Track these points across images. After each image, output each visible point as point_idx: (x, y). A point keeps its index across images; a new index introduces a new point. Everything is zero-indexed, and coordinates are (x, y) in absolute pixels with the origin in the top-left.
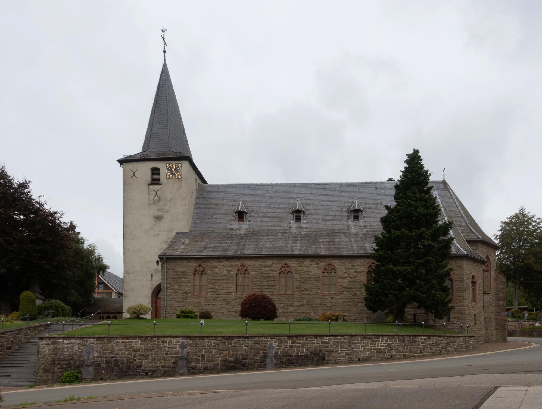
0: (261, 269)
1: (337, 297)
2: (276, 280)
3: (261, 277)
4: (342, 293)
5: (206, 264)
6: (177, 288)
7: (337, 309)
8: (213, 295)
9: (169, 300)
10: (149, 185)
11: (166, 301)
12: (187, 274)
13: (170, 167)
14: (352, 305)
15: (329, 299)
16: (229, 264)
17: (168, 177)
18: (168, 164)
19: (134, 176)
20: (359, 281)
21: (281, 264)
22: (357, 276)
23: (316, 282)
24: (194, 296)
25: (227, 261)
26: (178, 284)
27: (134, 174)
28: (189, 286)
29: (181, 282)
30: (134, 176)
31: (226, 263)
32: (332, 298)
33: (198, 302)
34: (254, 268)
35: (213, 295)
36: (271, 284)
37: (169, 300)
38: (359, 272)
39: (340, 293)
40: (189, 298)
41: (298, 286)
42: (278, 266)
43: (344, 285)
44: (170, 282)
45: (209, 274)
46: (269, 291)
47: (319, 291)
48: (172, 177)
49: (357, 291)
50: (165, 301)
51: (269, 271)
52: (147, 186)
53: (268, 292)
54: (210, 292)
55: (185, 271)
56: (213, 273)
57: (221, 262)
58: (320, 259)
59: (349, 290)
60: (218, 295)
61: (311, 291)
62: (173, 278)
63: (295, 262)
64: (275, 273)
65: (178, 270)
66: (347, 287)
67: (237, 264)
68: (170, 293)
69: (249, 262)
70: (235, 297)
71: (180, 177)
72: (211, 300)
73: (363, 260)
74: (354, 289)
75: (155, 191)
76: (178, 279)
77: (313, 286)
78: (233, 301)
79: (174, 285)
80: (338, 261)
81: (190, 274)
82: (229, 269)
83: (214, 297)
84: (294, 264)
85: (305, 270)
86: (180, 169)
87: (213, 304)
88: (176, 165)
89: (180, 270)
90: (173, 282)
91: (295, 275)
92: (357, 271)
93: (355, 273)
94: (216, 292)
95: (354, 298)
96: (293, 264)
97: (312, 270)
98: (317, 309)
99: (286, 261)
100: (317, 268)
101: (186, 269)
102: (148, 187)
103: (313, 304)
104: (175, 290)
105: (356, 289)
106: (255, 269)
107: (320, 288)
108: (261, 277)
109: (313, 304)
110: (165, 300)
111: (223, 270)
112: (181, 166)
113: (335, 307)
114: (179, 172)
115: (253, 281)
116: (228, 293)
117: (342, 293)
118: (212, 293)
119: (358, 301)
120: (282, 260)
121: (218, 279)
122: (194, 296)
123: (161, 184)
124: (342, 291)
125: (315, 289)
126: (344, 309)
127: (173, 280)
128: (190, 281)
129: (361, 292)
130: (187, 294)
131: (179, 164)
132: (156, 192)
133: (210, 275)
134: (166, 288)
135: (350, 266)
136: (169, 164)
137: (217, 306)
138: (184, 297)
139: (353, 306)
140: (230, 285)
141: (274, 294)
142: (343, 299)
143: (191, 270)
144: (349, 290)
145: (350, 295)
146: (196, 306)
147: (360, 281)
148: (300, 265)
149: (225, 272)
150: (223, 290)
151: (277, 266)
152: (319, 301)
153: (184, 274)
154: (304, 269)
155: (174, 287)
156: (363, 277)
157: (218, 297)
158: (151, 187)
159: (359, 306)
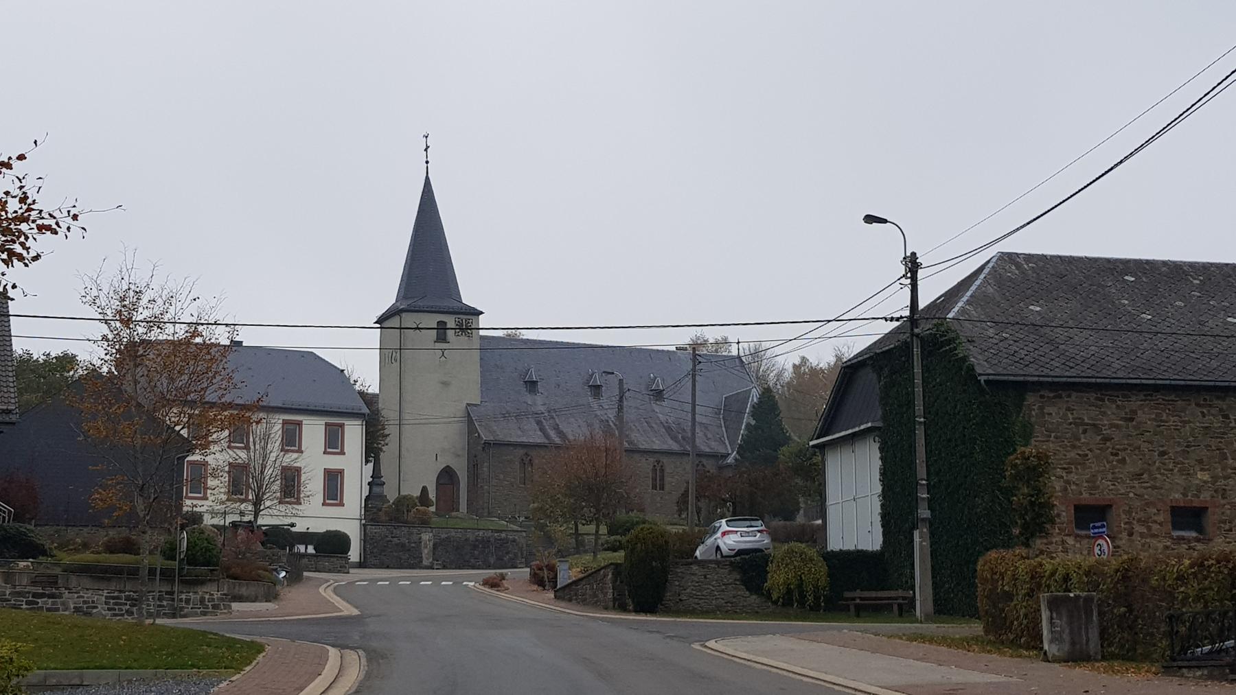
10: (435, 342)
15: (659, 498)
32: (661, 498)
52: (433, 343)
135: (678, 463)
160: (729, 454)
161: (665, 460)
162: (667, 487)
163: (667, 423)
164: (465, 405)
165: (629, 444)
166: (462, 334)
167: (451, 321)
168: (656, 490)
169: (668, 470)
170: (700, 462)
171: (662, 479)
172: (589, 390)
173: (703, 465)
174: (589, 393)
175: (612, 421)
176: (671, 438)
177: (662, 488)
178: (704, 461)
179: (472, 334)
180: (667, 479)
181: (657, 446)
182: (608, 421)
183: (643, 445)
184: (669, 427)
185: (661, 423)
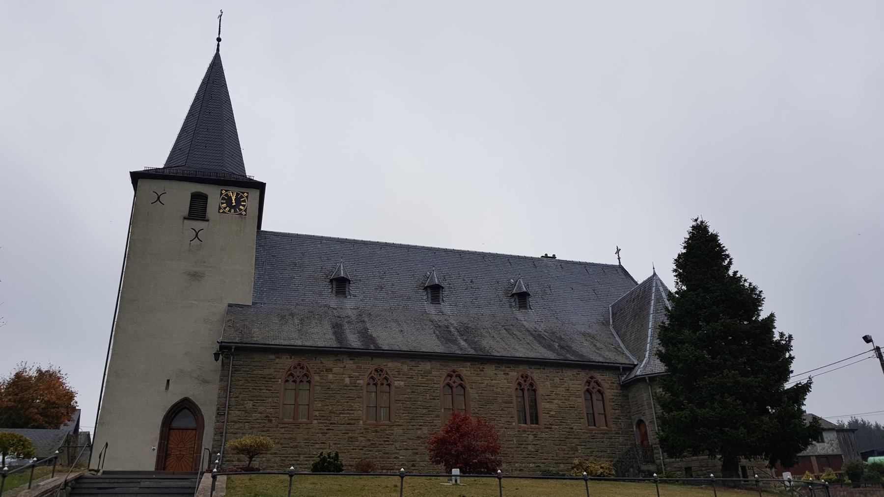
0: (413, 378)
1: (544, 435)
2: (438, 399)
3: (412, 392)
4: (551, 428)
5: (311, 364)
7: (546, 458)
8: (321, 423)
9: (232, 433)
10: (185, 218)
11: (226, 433)
12: (272, 380)
13: (226, 195)
14: (568, 449)
15: (531, 437)
16: (354, 366)
17: (221, 211)
20: (574, 407)
21: (446, 369)
22: (571, 398)
23: (506, 405)
24: (284, 426)
25: (351, 360)
27: (159, 198)
29: (258, 396)
30: (158, 202)
31: (349, 363)
32: (535, 436)
33: (291, 438)
34: (399, 374)
35: (321, 423)
36: (431, 406)
37: (232, 433)
38: (572, 391)
39: (547, 428)
40: (275, 429)
41: (476, 411)
42: (440, 374)
43: (552, 413)
44: (237, 395)
45: (316, 382)
46: (428, 419)
47: (513, 422)
48: (230, 211)
49: (573, 424)
50: (224, 434)
51: (426, 382)
53: (425, 421)
54: (316, 418)
56: (323, 381)
57: (339, 360)
58: (510, 365)
59: (561, 422)
60: (331, 424)
61: (500, 422)
62: (244, 387)
63: (468, 369)
64: (436, 386)
65: (255, 372)
66: (557, 416)
67: (369, 366)
68: (235, 419)
69: (390, 364)
70: (365, 429)
71: (244, 213)
72: (318, 433)
73: (575, 371)
74: (569, 421)
76: (254, 389)
77: (501, 412)
78: (360, 437)
80: (538, 371)
81: (280, 380)
82: (354, 374)
83: (323, 428)
84: (468, 371)
85: (487, 384)
86: (244, 201)
87: (322, 443)
88: (238, 194)
89: (260, 372)
90: (241, 396)
91: (471, 391)
92: (568, 390)
93: (567, 393)
94: (329, 418)
95: (570, 436)
96: (466, 371)
97: (498, 383)
98: (513, 457)
99: (454, 366)
100: (506, 381)
101: (272, 371)
102: (183, 222)
103: (505, 446)
104: (246, 412)
105: (572, 422)
106: (401, 376)
107: (513, 417)
108: (412, 392)
109: (505, 446)
110: (224, 432)
111: (344, 376)
112: (247, 197)
113: (541, 453)
114: (244, 206)
115: (398, 399)
116: (351, 421)
117: (551, 428)
118: (320, 419)
119: (577, 443)
120: (447, 364)
121: (334, 392)
122: (284, 426)
123: (208, 220)
124: (550, 424)
125: (505, 418)
126: (556, 458)
127: (243, 391)
128: (278, 395)
129: (580, 428)
130: (270, 421)
131: (243, 193)
133: (318, 384)
134: (229, 408)
135: (557, 380)
136: (226, 191)
137: (330, 446)
138: (264, 427)
139: (570, 453)
140: (356, 406)
141: (436, 426)
142: (553, 439)
143: (281, 374)
144: (561, 422)
145: (563, 431)
146: (287, 445)
147: (576, 407)
148: (477, 374)
149: (347, 381)
150: (341, 415)
151: (438, 373)
152: (515, 441)
154: (486, 382)
156: (579, 400)
157: (333, 428)
158: (186, 222)
159: (579, 451)
160: (636, 365)
161: (536, 374)
162: (543, 418)
163: (536, 331)
164: (227, 305)
165: (475, 349)
166: (230, 211)
167: (214, 195)
168: (526, 424)
169: (541, 391)
170: (592, 378)
171: (534, 405)
172: (425, 293)
173: (596, 382)
174: (425, 298)
175: (454, 327)
176: (544, 347)
177: (535, 420)
178: (598, 376)
179: (245, 211)
180: (543, 405)
181: (521, 352)
182: (447, 327)
183: (498, 352)
184: (539, 336)
185: (529, 331)
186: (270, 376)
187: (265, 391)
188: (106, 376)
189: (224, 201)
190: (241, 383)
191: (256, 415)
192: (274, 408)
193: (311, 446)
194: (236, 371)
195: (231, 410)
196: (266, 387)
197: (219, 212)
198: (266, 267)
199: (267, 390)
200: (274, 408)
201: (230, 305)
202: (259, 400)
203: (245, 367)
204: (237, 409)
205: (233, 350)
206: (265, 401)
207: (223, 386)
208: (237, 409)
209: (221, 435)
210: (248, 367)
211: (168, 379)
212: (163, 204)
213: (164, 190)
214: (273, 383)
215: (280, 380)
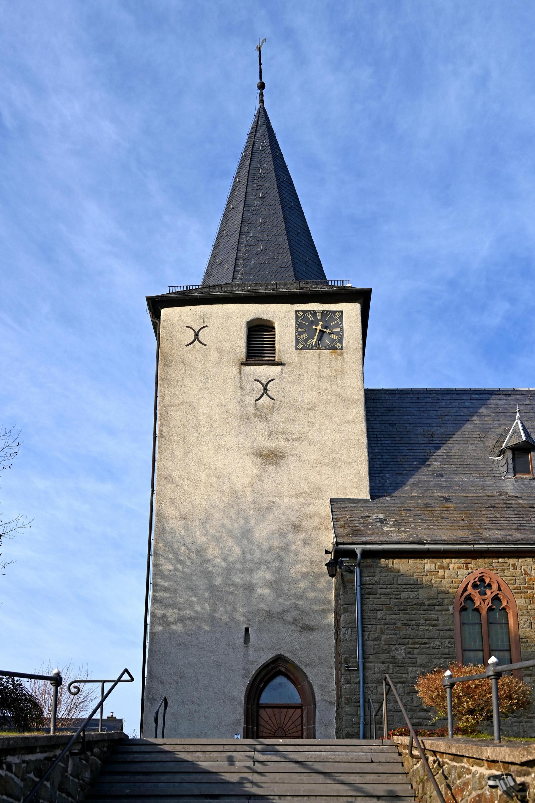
6: (404, 655)
10: (243, 364)
18: (301, 313)
19: (197, 342)
26: (404, 645)
27: (197, 335)
28: (447, 650)
29: (416, 637)
30: (197, 342)
44: (376, 635)
52: (237, 366)
55: (432, 599)
62: (386, 622)
65: (403, 595)
75: (262, 384)
76: (405, 624)
79: (393, 647)
81: (451, 608)
89: (413, 595)
90: (384, 637)
102: (240, 370)
104: (396, 664)
132: (265, 384)
153: (426, 607)
155: (393, 654)
158: (247, 369)
179: (341, 341)
186: (431, 602)
187: (427, 628)
188: (148, 627)
189: (304, 330)
190: (379, 614)
191: (415, 669)
192: (446, 656)
193: (526, 722)
194: (369, 594)
195: (369, 662)
196: (427, 620)
197: (297, 348)
198: (383, 442)
199: (430, 625)
200: (446, 656)
201: (333, 501)
202: (417, 643)
203: (385, 587)
204: (380, 660)
205: (359, 556)
206: (428, 646)
207: (348, 621)
208: (380, 660)
209: (358, 704)
210: (389, 586)
211: (246, 626)
212: (206, 345)
213: (204, 322)
214: (440, 613)
215: (451, 608)
